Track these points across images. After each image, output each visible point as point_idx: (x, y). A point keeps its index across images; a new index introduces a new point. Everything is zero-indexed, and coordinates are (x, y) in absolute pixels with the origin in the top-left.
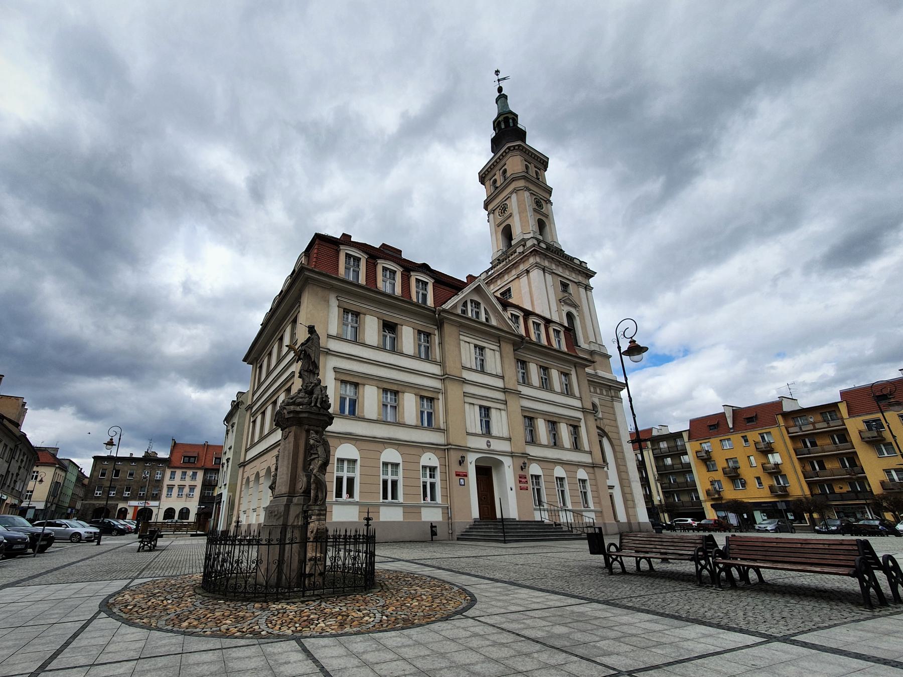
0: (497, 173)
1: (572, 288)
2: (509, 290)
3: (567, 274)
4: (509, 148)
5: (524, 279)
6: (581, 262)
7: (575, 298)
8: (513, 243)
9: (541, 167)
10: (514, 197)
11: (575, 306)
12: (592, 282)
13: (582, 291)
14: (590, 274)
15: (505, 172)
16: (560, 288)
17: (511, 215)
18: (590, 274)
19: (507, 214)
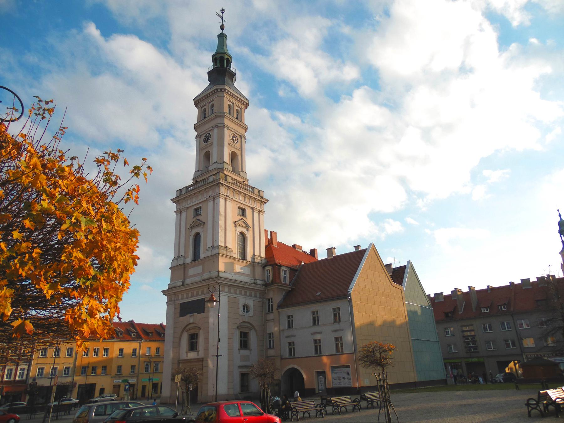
0: (207, 104)
1: (249, 212)
2: (201, 208)
3: (245, 202)
4: (217, 90)
5: (210, 204)
6: (259, 191)
7: (249, 221)
8: (210, 168)
9: (243, 107)
10: (216, 130)
11: (247, 227)
12: (266, 207)
13: (256, 215)
14: (264, 201)
15: (213, 106)
16: (240, 212)
17: (212, 144)
18: (264, 201)
19: (209, 142)
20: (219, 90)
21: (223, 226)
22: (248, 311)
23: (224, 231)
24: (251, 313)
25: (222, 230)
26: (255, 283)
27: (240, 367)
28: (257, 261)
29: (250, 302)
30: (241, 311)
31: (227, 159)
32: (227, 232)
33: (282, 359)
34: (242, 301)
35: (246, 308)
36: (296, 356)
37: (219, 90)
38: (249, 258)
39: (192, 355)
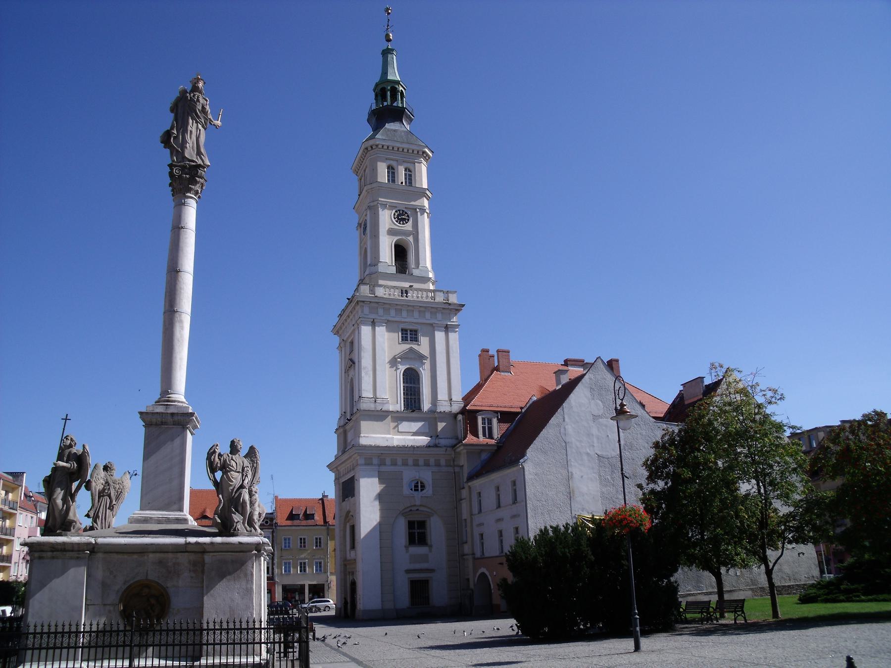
20: (370, 149)
21: (370, 368)
22: (423, 487)
23: (371, 373)
24: (429, 491)
25: (366, 373)
26: (436, 446)
27: (408, 571)
28: (440, 409)
29: (426, 476)
30: (406, 491)
31: (387, 255)
32: (378, 373)
33: (475, 559)
34: (409, 475)
35: (419, 486)
36: (486, 555)
37: (370, 149)
38: (426, 406)
39: (353, 553)
